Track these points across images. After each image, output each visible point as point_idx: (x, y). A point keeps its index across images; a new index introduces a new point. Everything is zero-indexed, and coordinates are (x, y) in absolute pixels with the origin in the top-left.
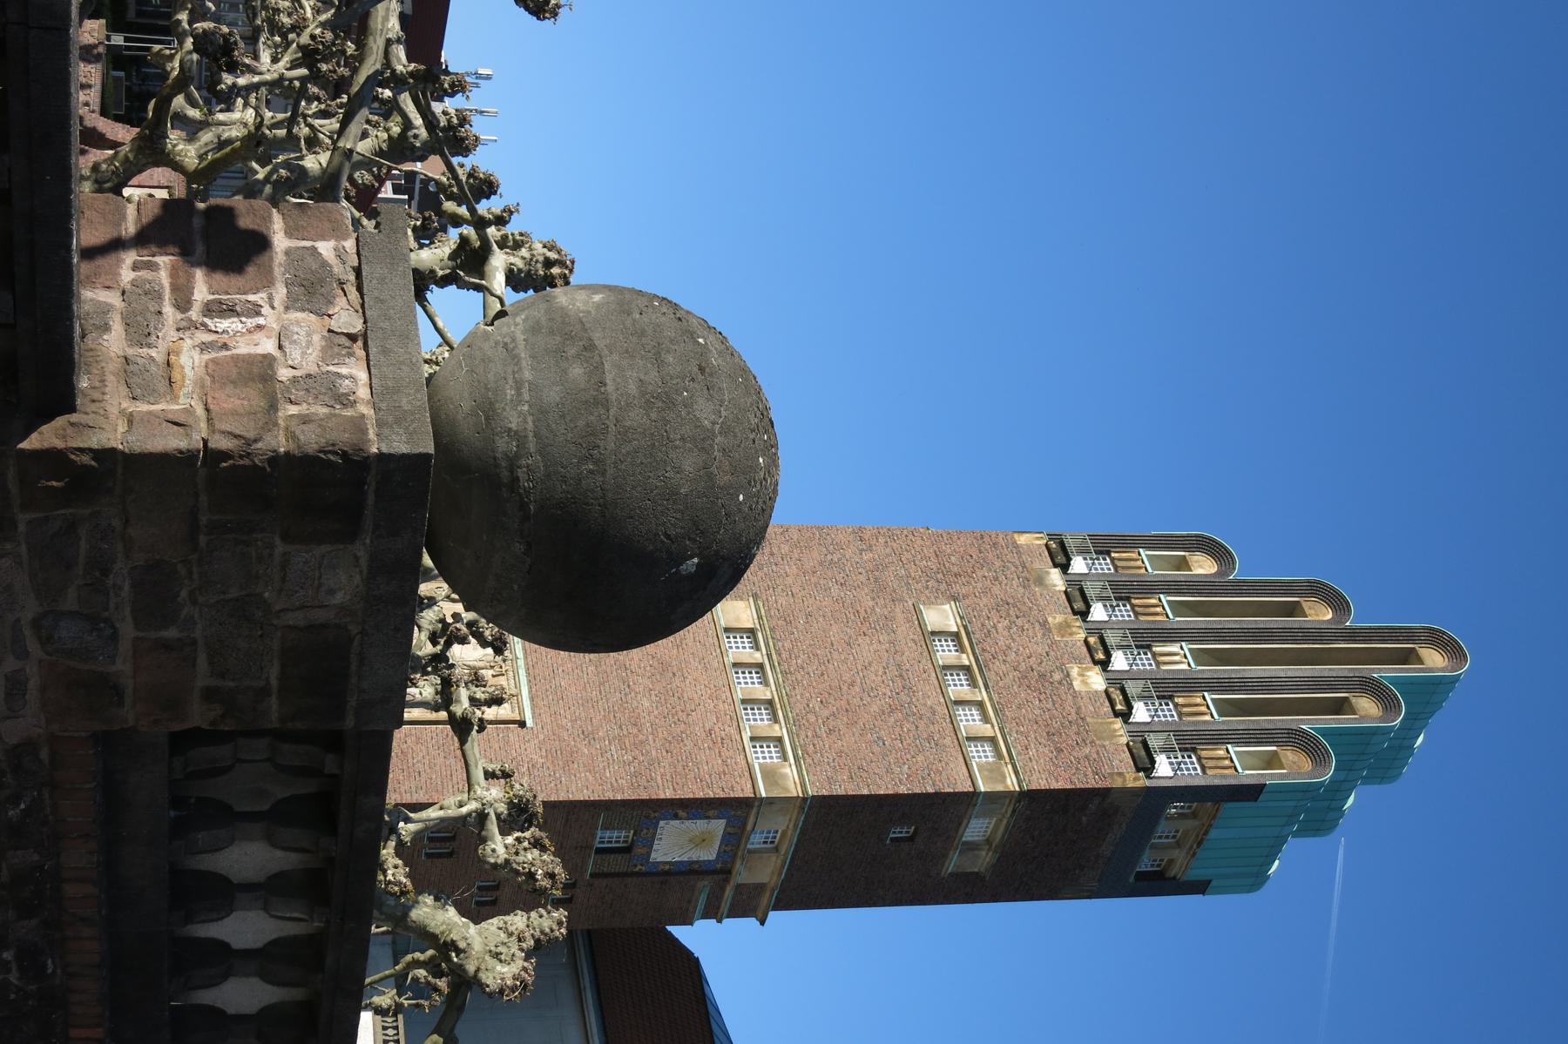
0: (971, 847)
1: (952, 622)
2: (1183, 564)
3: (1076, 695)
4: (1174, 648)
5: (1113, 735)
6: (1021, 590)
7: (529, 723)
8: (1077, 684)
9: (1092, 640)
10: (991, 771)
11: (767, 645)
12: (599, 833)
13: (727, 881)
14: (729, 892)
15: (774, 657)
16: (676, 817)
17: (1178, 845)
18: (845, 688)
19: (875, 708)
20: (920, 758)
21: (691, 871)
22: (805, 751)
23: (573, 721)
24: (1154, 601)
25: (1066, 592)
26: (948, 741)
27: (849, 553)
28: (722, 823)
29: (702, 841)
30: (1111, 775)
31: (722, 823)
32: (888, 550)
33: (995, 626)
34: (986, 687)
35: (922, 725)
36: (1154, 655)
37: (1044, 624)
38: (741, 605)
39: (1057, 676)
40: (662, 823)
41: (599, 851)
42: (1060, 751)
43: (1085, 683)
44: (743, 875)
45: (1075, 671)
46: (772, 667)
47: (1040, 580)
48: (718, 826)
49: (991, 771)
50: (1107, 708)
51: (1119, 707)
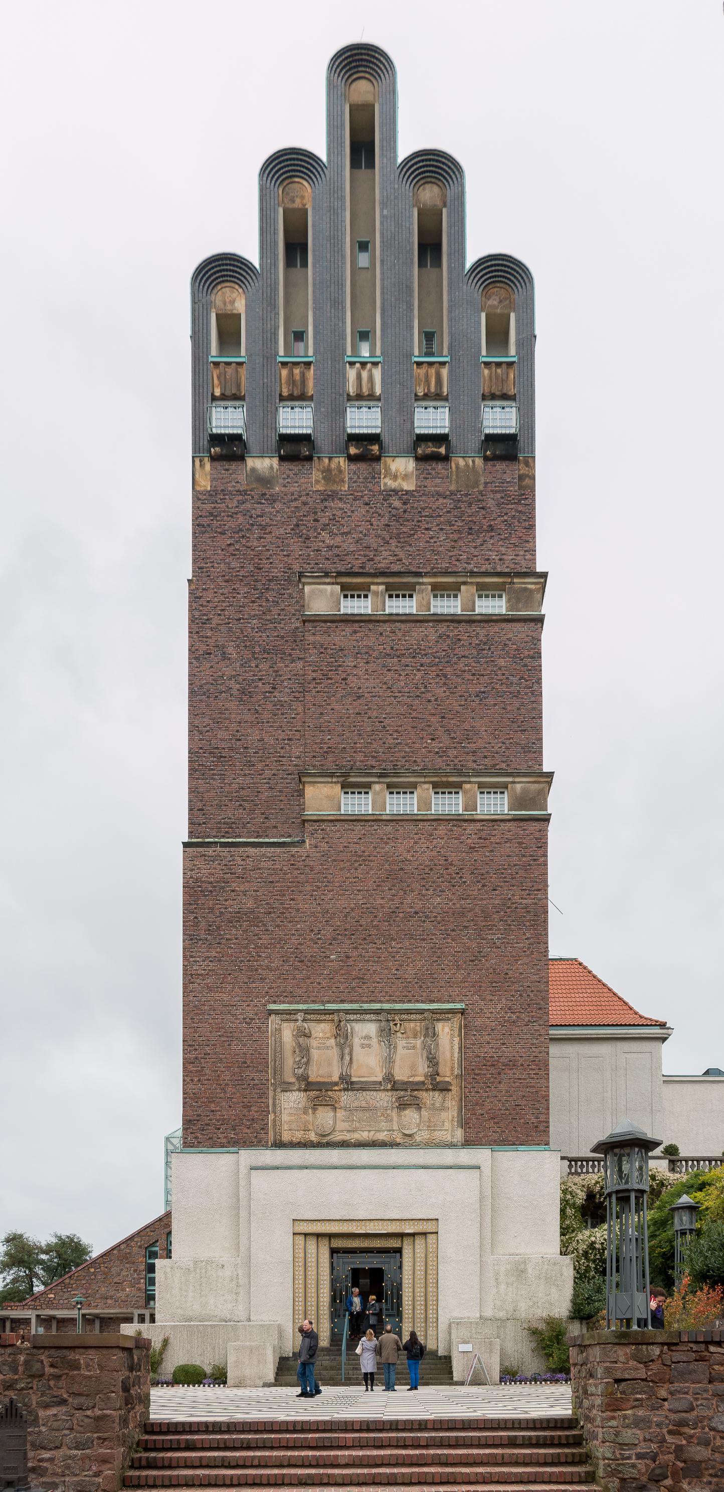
6: (278, 506)
10: (518, 600)
18: (414, 714)
19: (440, 691)
23: (459, 968)
26: (482, 632)
27: (228, 672)
32: (223, 629)
33: (330, 548)
34: (418, 574)
35: (460, 652)
38: (309, 791)
39: (397, 503)
42: (491, 528)
43: (406, 477)
45: (388, 483)
49: (518, 600)
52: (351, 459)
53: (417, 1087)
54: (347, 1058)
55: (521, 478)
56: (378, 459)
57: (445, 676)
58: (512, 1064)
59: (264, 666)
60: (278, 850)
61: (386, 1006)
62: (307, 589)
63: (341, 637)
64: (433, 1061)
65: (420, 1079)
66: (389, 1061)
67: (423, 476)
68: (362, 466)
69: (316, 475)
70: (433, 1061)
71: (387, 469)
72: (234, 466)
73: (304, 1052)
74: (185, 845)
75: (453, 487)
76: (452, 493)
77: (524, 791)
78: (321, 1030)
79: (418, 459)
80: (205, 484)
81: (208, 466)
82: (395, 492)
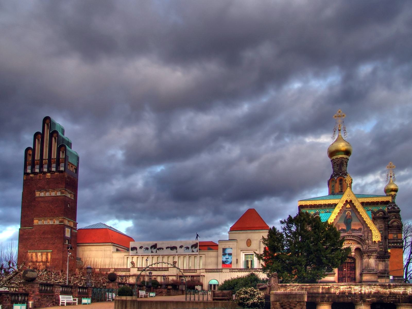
1: (39, 192)
5: (57, 175)
7: (51, 251)
8: (49, 177)
9: (42, 173)
12: (66, 243)
22: (58, 217)
25: (34, 175)
28: (66, 228)
31: (66, 228)
33: (39, 187)
37: (39, 179)
43: (49, 176)
45: (47, 177)
46: (45, 219)
47: (32, 178)
48: (67, 229)
50: (53, 174)
51: (53, 173)
52: (42, 174)
55: (64, 175)
60: (30, 229)
61: (42, 251)
64: (47, 258)
67: (51, 176)
68: (44, 175)
70: (47, 258)
71: (47, 175)
73: (32, 257)
74: (19, 229)
75: (55, 177)
79: (51, 174)
80: (25, 179)
81: (25, 176)
82: (48, 178)
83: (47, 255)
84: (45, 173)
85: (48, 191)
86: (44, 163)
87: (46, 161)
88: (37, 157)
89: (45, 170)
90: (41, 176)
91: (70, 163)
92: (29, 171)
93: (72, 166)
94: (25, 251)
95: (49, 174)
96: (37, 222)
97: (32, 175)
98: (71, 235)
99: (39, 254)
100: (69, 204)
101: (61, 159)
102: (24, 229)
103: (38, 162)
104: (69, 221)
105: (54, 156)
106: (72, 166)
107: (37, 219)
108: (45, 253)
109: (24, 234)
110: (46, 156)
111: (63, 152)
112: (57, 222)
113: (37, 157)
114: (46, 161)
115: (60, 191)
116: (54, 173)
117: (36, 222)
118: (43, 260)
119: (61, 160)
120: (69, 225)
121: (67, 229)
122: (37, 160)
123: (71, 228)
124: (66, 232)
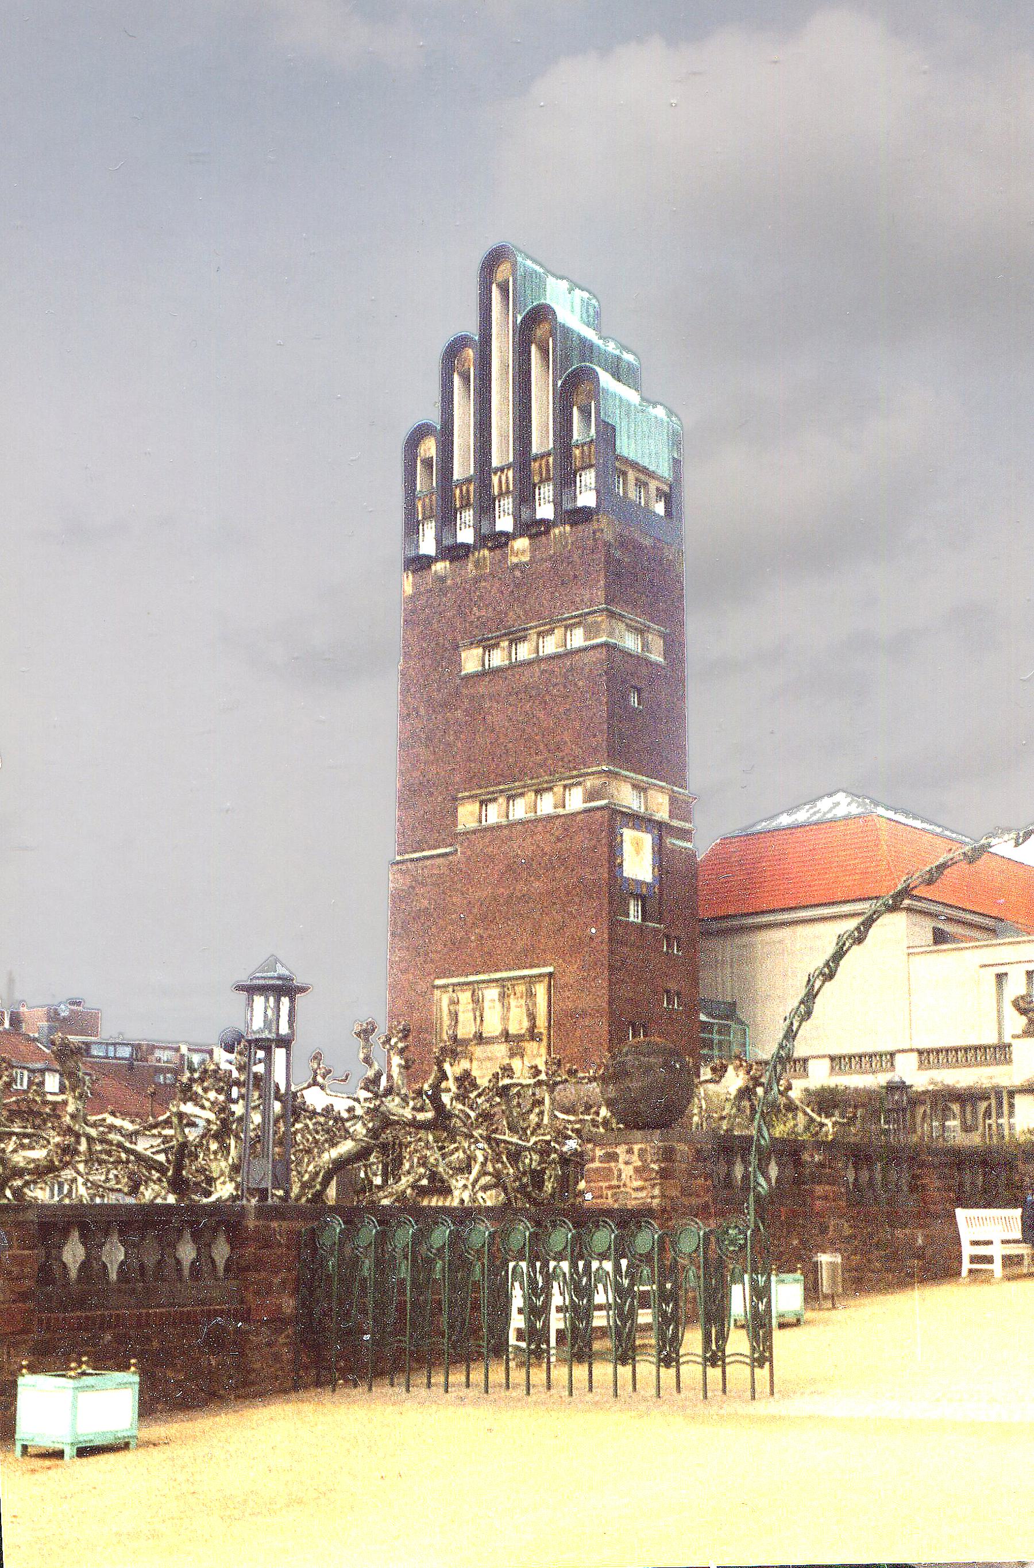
0: (645, 646)
2: (428, 463)
3: (532, 561)
4: (495, 479)
7: (550, 969)
8: (525, 558)
11: (493, 793)
12: (631, 919)
13: (667, 825)
14: (675, 823)
15: (501, 787)
16: (621, 865)
17: (646, 484)
19: (541, 715)
20: (580, 683)
21: (660, 851)
22: (575, 768)
24: (458, 492)
29: (637, 844)
30: (595, 540)
36: (501, 494)
37: (476, 580)
38: (460, 809)
39: (518, 573)
40: (625, 875)
41: (643, 920)
43: (524, 552)
44: (662, 814)
45: (515, 560)
46: (509, 789)
47: (442, 579)
48: (629, 835)
50: (544, 538)
52: (491, 549)
53: (520, 1038)
54: (478, 1019)
56: (506, 544)
57: (545, 702)
58: (584, 1014)
59: (439, 717)
62: (463, 655)
63: (482, 688)
64: (532, 1017)
65: (523, 1031)
66: (505, 1019)
67: (533, 549)
68: (498, 552)
69: (470, 566)
70: (532, 1017)
71: (512, 547)
72: (425, 572)
73: (455, 1017)
76: (552, 557)
77: (592, 786)
78: (465, 997)
82: (516, 566)
83: (531, 995)
84: (500, 541)
85: (522, 634)
86: (496, 491)
87: (504, 478)
88: (463, 467)
89: (505, 523)
90: (484, 558)
91: (626, 461)
92: (428, 546)
93: (642, 477)
94: (422, 987)
95: (522, 543)
96: (472, 814)
97: (440, 567)
98: (661, 867)
99: (491, 994)
100: (639, 691)
101: (577, 446)
102: (412, 860)
103: (468, 491)
104: (645, 790)
105: (542, 440)
106: (642, 477)
107: (471, 797)
108: (521, 988)
109: (413, 888)
110: (501, 453)
111: (586, 413)
112: (576, 801)
113: (463, 467)
114: (504, 478)
115: (579, 624)
116: (547, 532)
117: (467, 815)
118: (513, 1030)
119: (577, 452)
120: (642, 810)
121: (629, 835)
122: (460, 484)
123: (659, 829)
124: (628, 849)
